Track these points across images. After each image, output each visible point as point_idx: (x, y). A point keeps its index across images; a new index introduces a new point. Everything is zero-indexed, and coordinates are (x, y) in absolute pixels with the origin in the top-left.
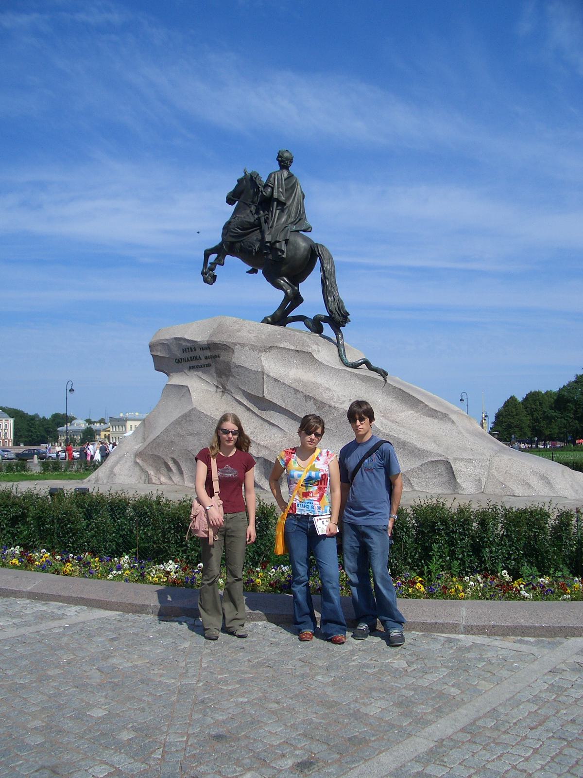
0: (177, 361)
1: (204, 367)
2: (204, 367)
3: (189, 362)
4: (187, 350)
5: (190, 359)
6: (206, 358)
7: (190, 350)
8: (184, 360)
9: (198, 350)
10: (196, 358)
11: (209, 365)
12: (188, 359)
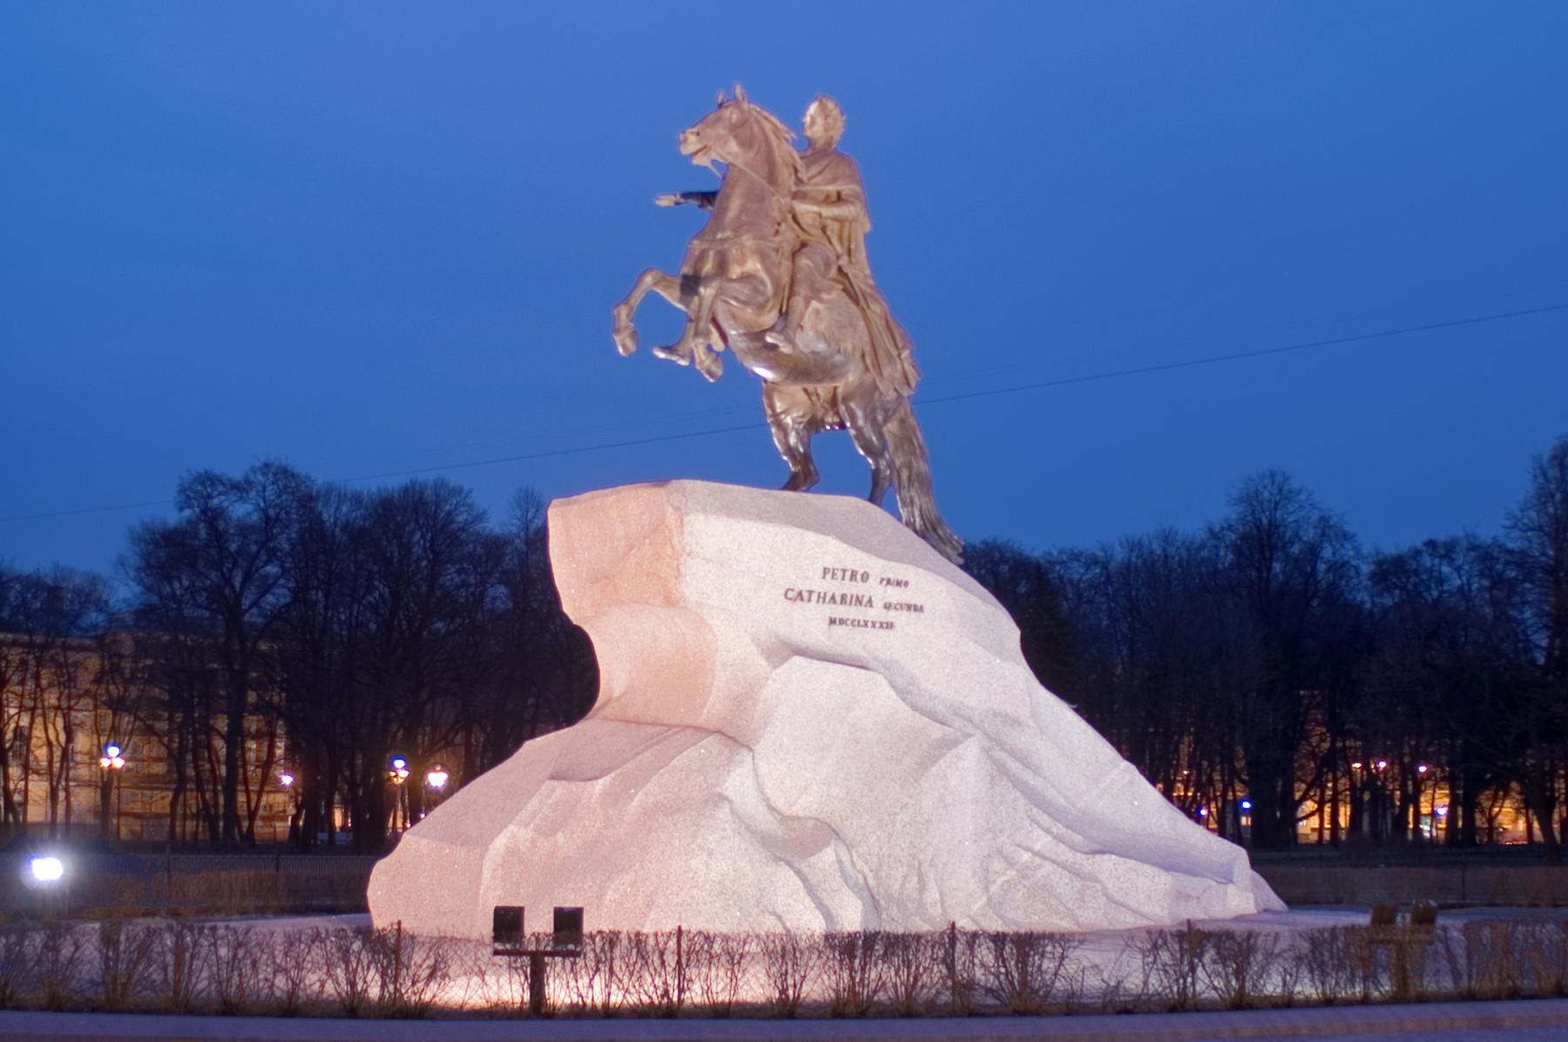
0: (790, 594)
1: (874, 625)
2: (874, 625)
3: (832, 606)
4: (839, 574)
5: (838, 599)
6: (887, 606)
7: (848, 574)
8: (822, 598)
9: (873, 581)
10: (859, 601)
11: (890, 626)
12: (833, 597)
